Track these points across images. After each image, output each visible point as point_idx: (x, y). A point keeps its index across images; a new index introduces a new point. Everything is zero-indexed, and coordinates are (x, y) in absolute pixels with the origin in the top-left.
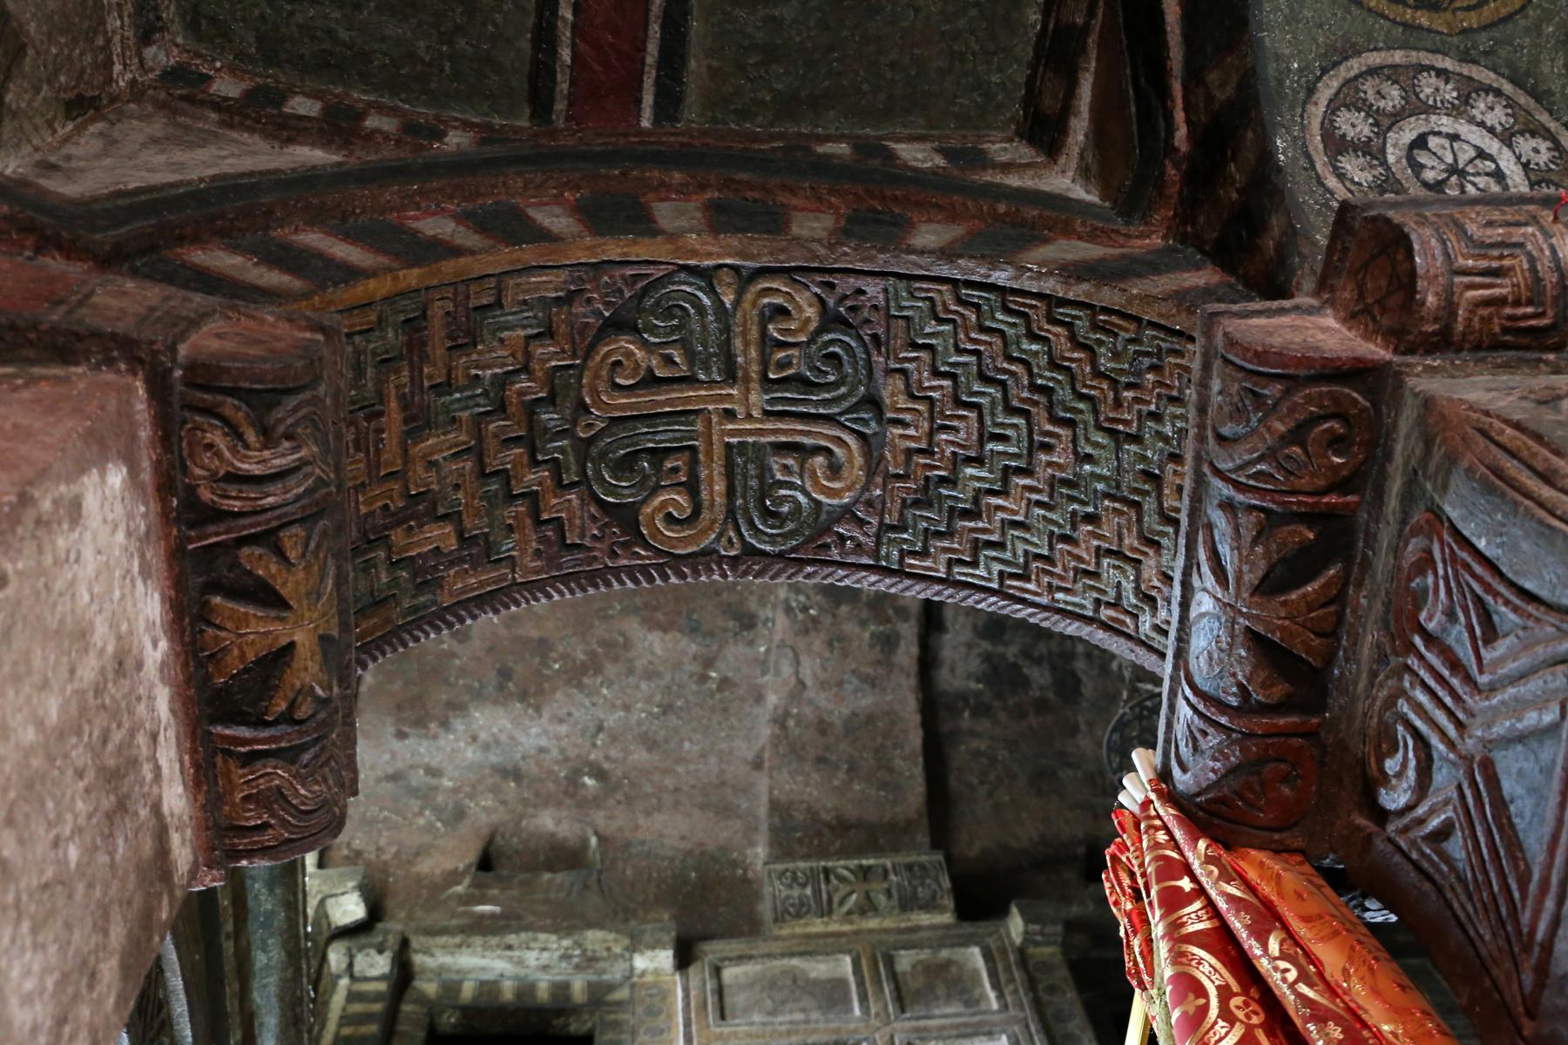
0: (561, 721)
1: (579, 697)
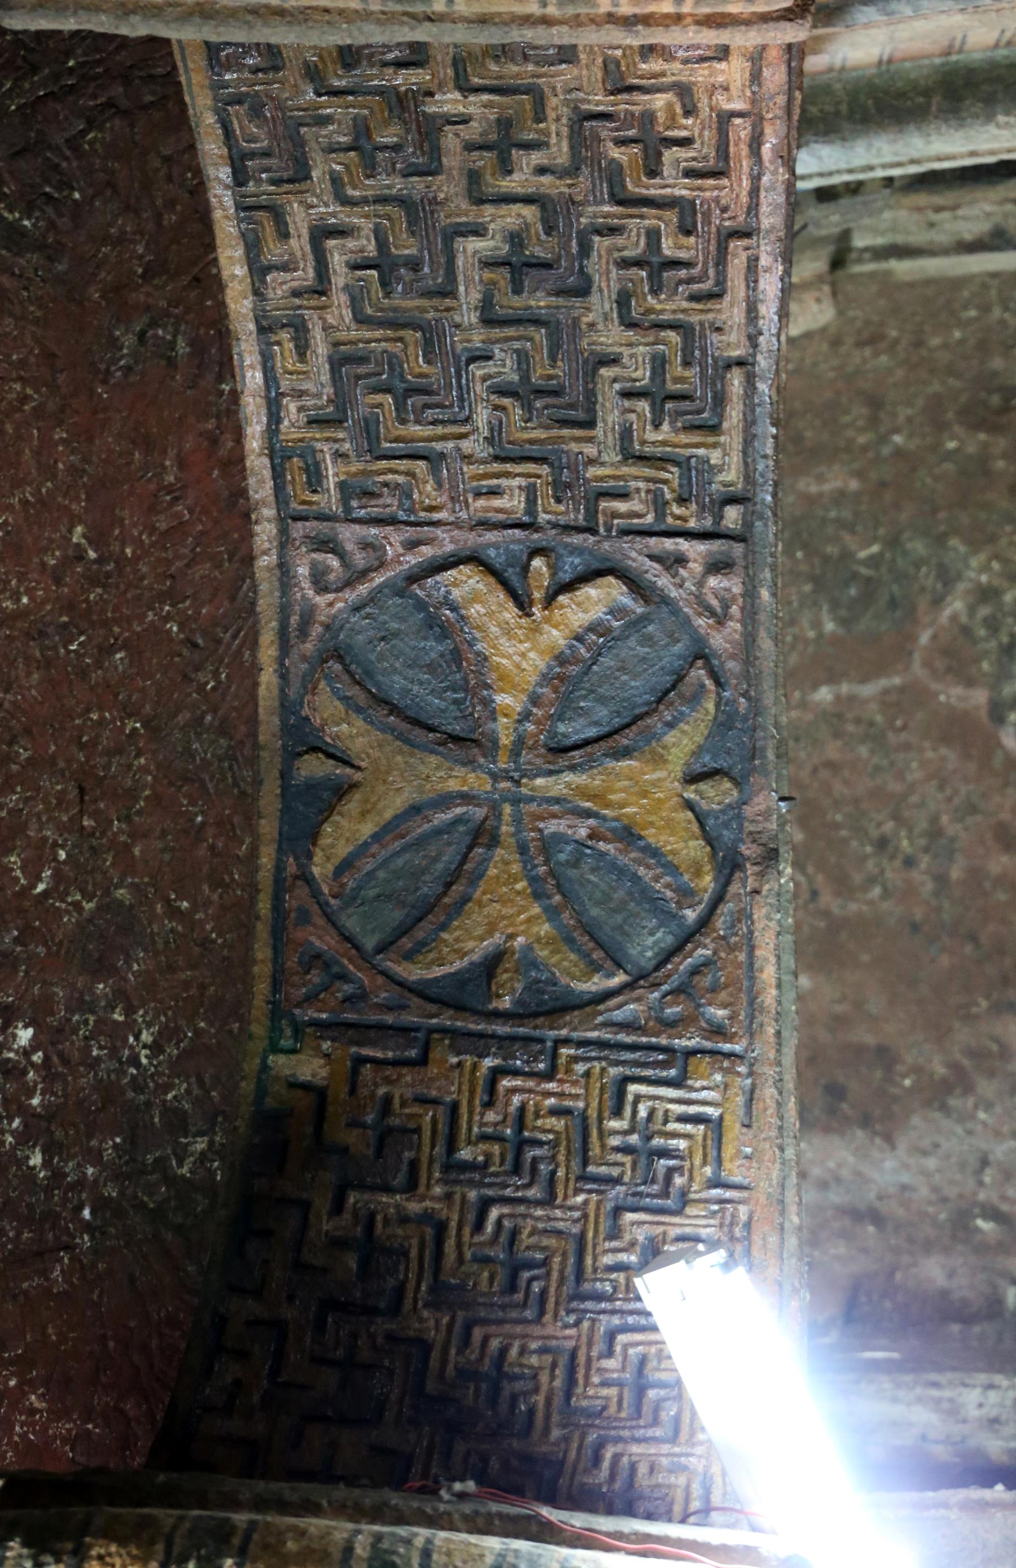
0: (925, 1153)
1: (945, 1123)
